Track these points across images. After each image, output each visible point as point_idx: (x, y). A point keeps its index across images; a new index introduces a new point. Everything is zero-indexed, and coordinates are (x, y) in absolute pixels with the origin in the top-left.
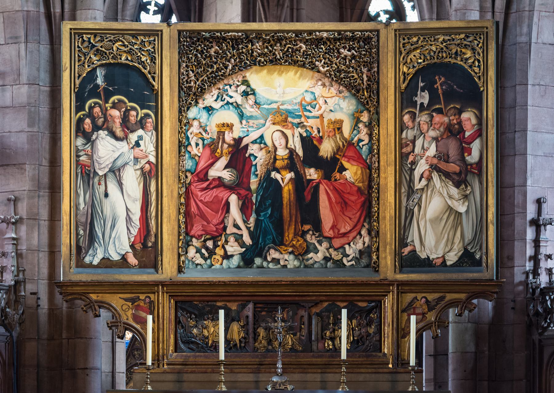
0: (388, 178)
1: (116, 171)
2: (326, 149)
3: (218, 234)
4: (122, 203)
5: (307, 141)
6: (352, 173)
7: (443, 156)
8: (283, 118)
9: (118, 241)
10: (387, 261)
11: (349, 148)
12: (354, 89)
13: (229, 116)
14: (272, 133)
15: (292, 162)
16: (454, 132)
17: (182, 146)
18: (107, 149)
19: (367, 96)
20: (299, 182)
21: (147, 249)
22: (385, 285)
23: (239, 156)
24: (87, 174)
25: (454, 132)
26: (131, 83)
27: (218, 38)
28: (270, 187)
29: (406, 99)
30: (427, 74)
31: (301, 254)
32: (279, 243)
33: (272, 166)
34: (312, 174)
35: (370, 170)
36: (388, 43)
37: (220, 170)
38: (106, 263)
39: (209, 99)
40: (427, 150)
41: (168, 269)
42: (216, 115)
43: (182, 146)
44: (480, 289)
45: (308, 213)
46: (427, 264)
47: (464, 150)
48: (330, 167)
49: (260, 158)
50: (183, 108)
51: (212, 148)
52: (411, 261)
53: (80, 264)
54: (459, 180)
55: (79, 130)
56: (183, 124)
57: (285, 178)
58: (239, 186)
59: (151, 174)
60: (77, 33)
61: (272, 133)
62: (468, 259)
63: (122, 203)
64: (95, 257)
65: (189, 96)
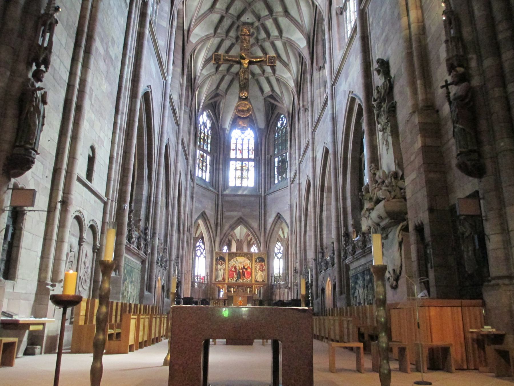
0: (253, 271)
1: (220, 269)
2: (246, 267)
3: (233, 277)
4: (221, 273)
5: (244, 266)
6: (249, 270)
7: (260, 268)
8: (241, 263)
9: (220, 278)
10: (253, 281)
11: (249, 267)
12: (249, 260)
13: (234, 263)
14: (239, 265)
15: (242, 269)
16: (262, 265)
17: (229, 266)
18: (219, 267)
19: (251, 261)
20: (243, 271)
21: (224, 279)
22: (253, 284)
23: (235, 268)
24: (217, 270)
25: (262, 265)
26: (222, 259)
27: (233, 253)
28: (239, 272)
29: (256, 261)
30: (258, 258)
31: (243, 280)
32: (240, 279)
33: (239, 269)
34: (244, 270)
35: (251, 270)
36: (253, 255)
37: (233, 270)
38: (219, 281)
39: (232, 261)
40: (258, 267)
41: (227, 281)
42: (233, 262)
43: (229, 266)
44: (264, 285)
45: (244, 275)
46: (258, 282)
47: (263, 267)
48: (246, 269)
49: (238, 268)
50: (229, 262)
51: (232, 267)
52: (256, 281)
53: (216, 281)
54: (262, 271)
55: (216, 264)
56: (229, 264)
57: (241, 271)
58: (235, 271)
59: (224, 270)
60: (216, 253)
61: (239, 265)
62: (263, 281)
63: (221, 273)
64: (217, 280)
65: (229, 260)
